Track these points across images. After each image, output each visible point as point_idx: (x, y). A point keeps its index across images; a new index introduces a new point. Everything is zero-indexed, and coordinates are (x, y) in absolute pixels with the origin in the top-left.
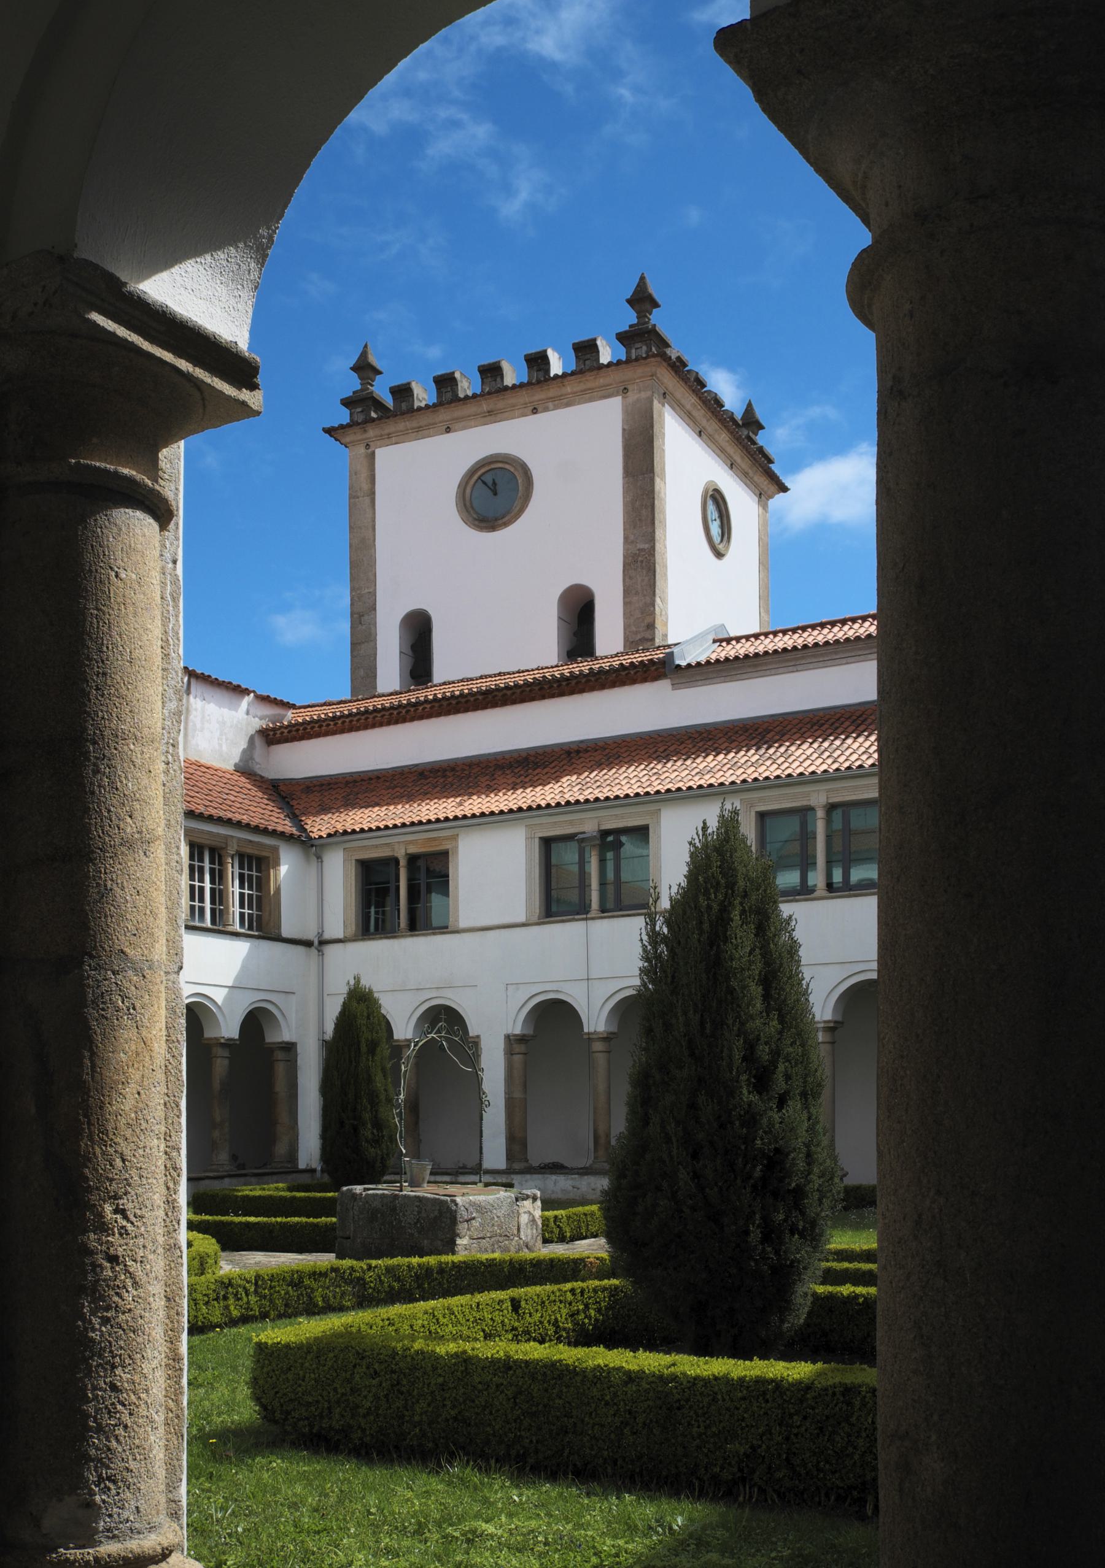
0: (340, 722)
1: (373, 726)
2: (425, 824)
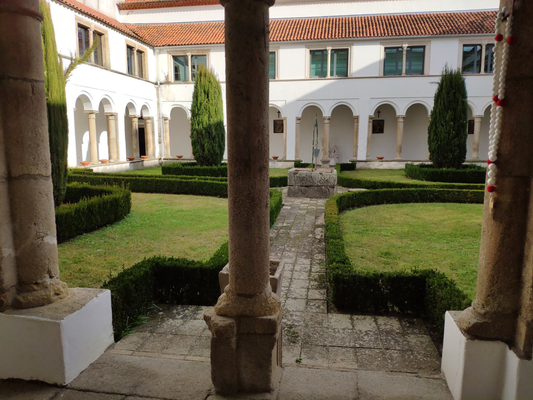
0: (148, 4)
1: (161, 7)
2: (196, 44)
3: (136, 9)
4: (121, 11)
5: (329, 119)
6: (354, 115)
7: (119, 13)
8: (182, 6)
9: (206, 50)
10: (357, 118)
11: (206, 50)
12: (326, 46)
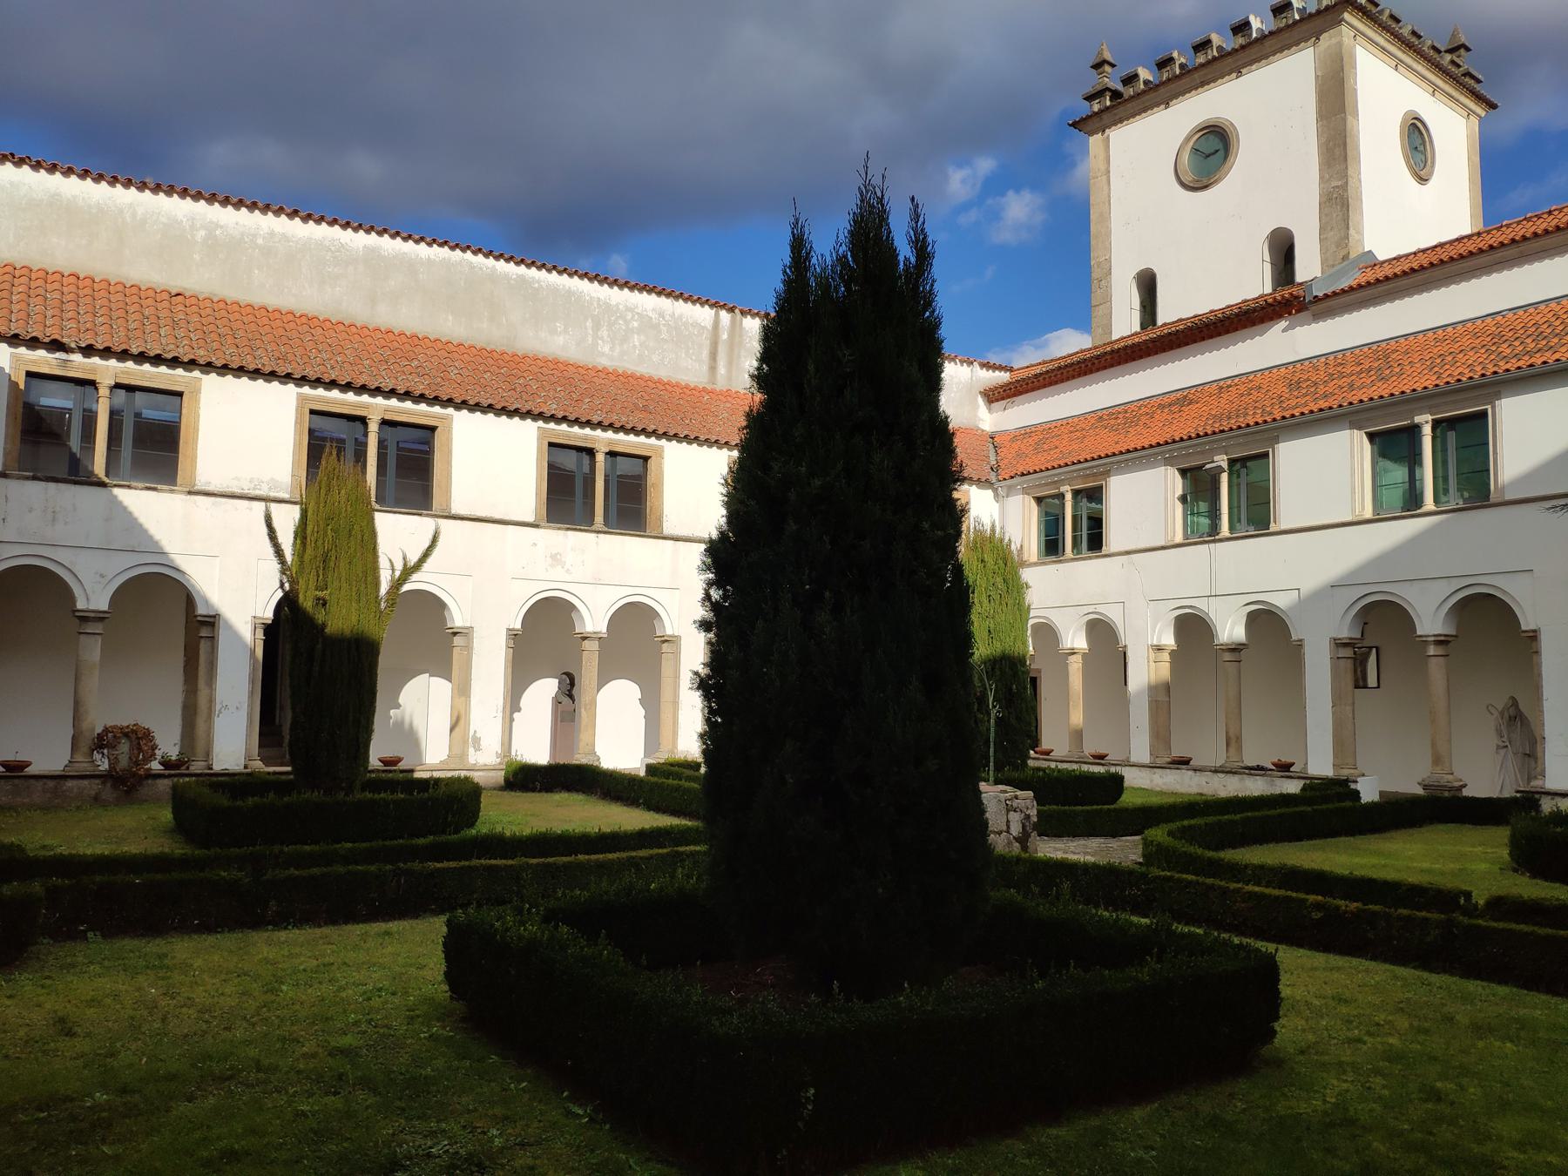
0: (1041, 378)
1: (1068, 379)
3: (1021, 393)
4: (993, 405)
5: (1438, 643)
6: (1524, 628)
7: (990, 410)
8: (1112, 366)
9: (1102, 474)
10: (1534, 636)
11: (1102, 474)
12: (1413, 414)
